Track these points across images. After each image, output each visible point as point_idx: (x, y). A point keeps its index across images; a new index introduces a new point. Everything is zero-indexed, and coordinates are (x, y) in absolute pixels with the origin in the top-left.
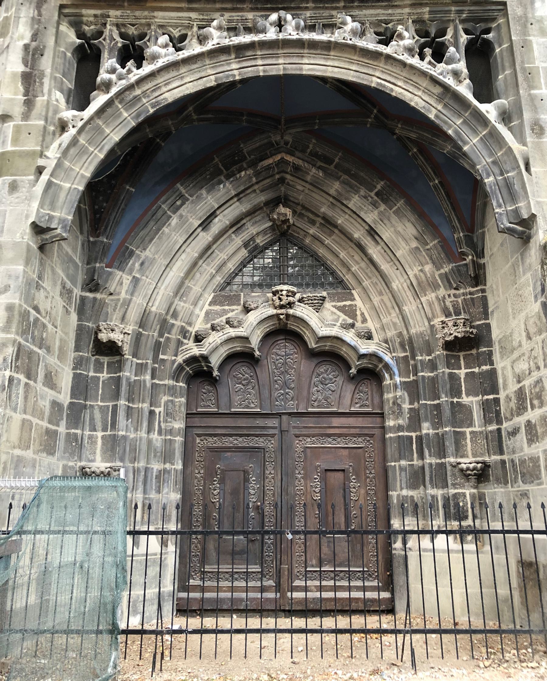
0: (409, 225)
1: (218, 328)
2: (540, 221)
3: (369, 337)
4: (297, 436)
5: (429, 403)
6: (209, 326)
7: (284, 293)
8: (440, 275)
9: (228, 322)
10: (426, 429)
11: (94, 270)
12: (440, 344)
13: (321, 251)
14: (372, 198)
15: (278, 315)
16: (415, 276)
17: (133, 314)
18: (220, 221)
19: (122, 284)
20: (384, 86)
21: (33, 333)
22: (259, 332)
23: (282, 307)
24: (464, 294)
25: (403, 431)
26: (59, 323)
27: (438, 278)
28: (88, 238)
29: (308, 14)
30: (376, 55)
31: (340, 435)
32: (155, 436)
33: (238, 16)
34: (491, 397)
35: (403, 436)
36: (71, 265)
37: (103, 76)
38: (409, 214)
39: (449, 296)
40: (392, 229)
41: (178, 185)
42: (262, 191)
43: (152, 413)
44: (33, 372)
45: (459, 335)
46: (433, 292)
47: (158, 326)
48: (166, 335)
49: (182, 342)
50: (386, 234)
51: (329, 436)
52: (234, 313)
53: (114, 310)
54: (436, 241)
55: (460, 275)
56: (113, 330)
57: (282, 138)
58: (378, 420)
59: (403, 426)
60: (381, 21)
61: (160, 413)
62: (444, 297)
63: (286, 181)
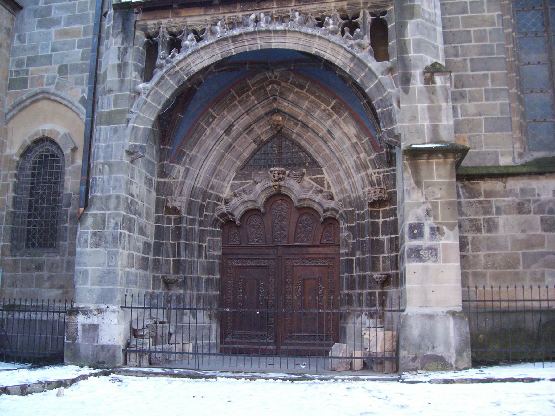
0: (352, 128)
1: (238, 195)
2: (403, 137)
3: (331, 198)
4: (288, 259)
5: (361, 239)
6: (232, 193)
7: (276, 172)
8: (370, 160)
9: (244, 191)
10: (358, 255)
11: (164, 166)
12: (367, 204)
13: (303, 143)
14: (329, 110)
15: (274, 186)
16: (354, 161)
17: (186, 190)
18: (237, 128)
19: (179, 172)
20: (319, 53)
21: (130, 208)
22: (263, 197)
23: (276, 181)
24: (383, 172)
25: (347, 256)
26: (145, 199)
27: (368, 162)
28: (159, 147)
29: (274, 11)
30: (313, 36)
31: (312, 259)
32: (203, 259)
33: (233, 16)
34: (394, 236)
35: (347, 259)
36: (150, 165)
37: (159, 61)
38: (351, 120)
39: (375, 173)
40: (341, 131)
41: (210, 109)
42: (262, 108)
43: (200, 247)
44: (132, 229)
45: (376, 199)
46: (364, 171)
47: (201, 196)
48: (207, 200)
49: (217, 204)
50: (337, 133)
51: (307, 259)
52: (248, 184)
53: (176, 188)
54: (367, 139)
55: (381, 160)
56: (175, 201)
57: (273, 74)
58: (337, 249)
59: (348, 253)
60: (318, 11)
61: (205, 246)
62: (371, 174)
63: (277, 100)
